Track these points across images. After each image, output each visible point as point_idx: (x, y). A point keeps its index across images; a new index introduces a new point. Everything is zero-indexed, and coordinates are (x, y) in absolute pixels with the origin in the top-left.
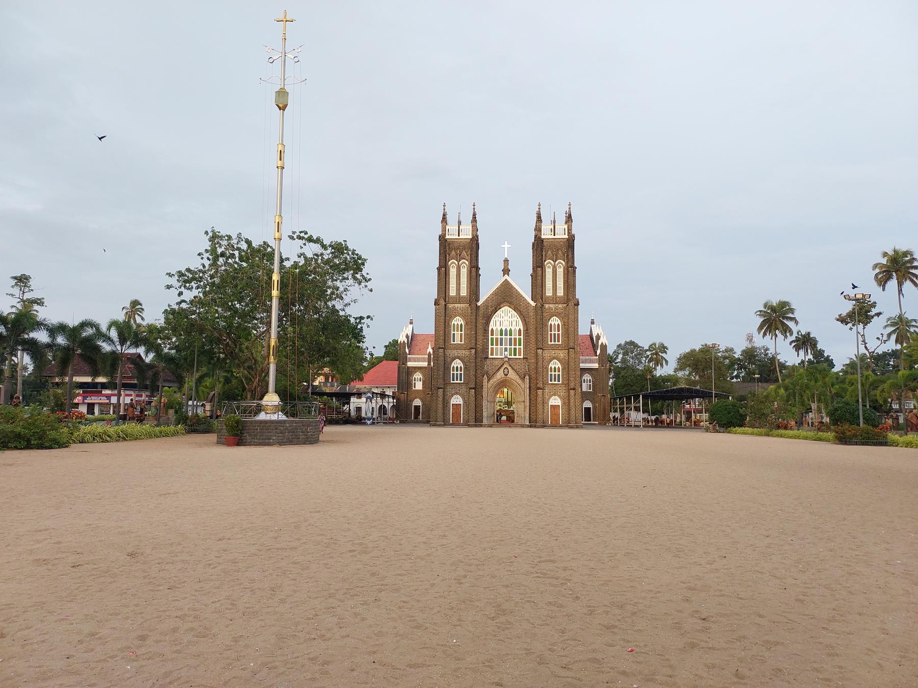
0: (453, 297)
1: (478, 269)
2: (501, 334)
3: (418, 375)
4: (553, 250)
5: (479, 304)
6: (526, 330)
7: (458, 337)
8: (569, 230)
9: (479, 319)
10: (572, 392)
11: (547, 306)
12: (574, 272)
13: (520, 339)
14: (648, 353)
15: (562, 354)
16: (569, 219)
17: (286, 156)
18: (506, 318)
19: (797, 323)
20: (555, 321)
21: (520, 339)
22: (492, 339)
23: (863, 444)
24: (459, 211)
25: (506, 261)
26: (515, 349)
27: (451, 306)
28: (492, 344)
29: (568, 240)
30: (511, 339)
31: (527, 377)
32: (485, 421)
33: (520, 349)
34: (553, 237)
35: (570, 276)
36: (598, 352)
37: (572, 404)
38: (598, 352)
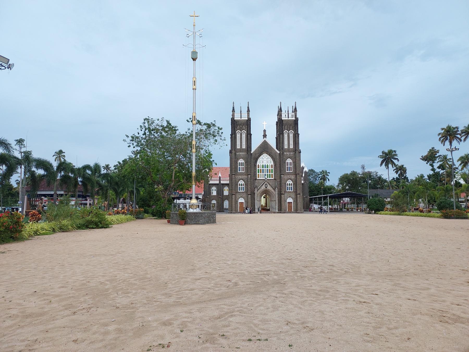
0: (238, 149)
1: (251, 135)
2: (263, 168)
3: (214, 188)
4: (287, 126)
6: (275, 165)
7: (241, 169)
8: (296, 115)
9: (252, 159)
10: (298, 195)
11: (285, 153)
12: (299, 136)
13: (272, 170)
14: (320, 175)
15: (293, 177)
16: (295, 110)
17: (197, 83)
18: (265, 159)
19: (398, 160)
20: (289, 161)
21: (272, 170)
22: (258, 170)
23: (457, 218)
24: (241, 106)
25: (265, 131)
26: (270, 175)
27: (238, 153)
28: (258, 172)
29: (295, 120)
30: (267, 170)
32: (256, 210)
33: (272, 175)
34: (287, 119)
35: (297, 139)
36: (303, 175)
37: (298, 201)
38: (303, 175)
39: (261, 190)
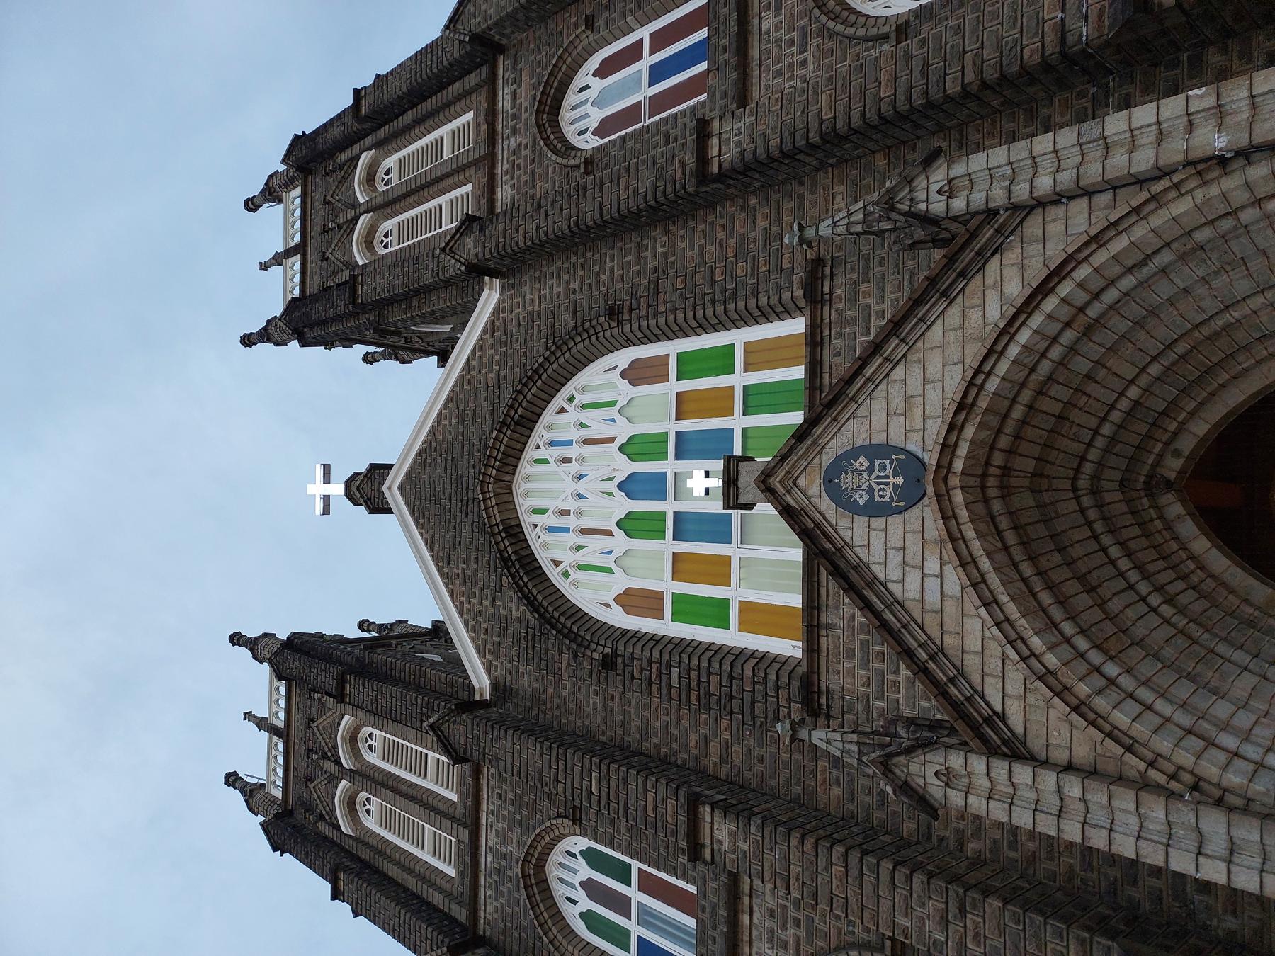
5: (481, 679)
6: (619, 321)
11: (504, 193)
22: (687, 609)
28: (717, 613)
31: (930, 193)
39: (971, 637)
